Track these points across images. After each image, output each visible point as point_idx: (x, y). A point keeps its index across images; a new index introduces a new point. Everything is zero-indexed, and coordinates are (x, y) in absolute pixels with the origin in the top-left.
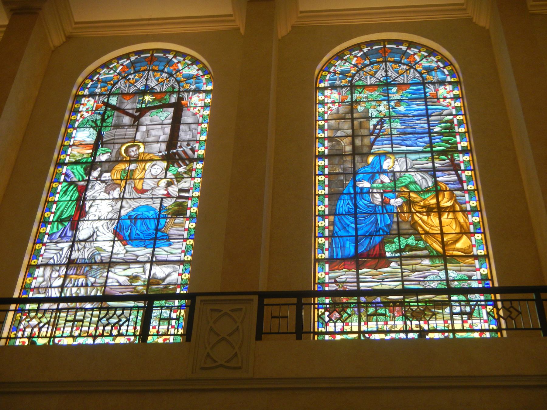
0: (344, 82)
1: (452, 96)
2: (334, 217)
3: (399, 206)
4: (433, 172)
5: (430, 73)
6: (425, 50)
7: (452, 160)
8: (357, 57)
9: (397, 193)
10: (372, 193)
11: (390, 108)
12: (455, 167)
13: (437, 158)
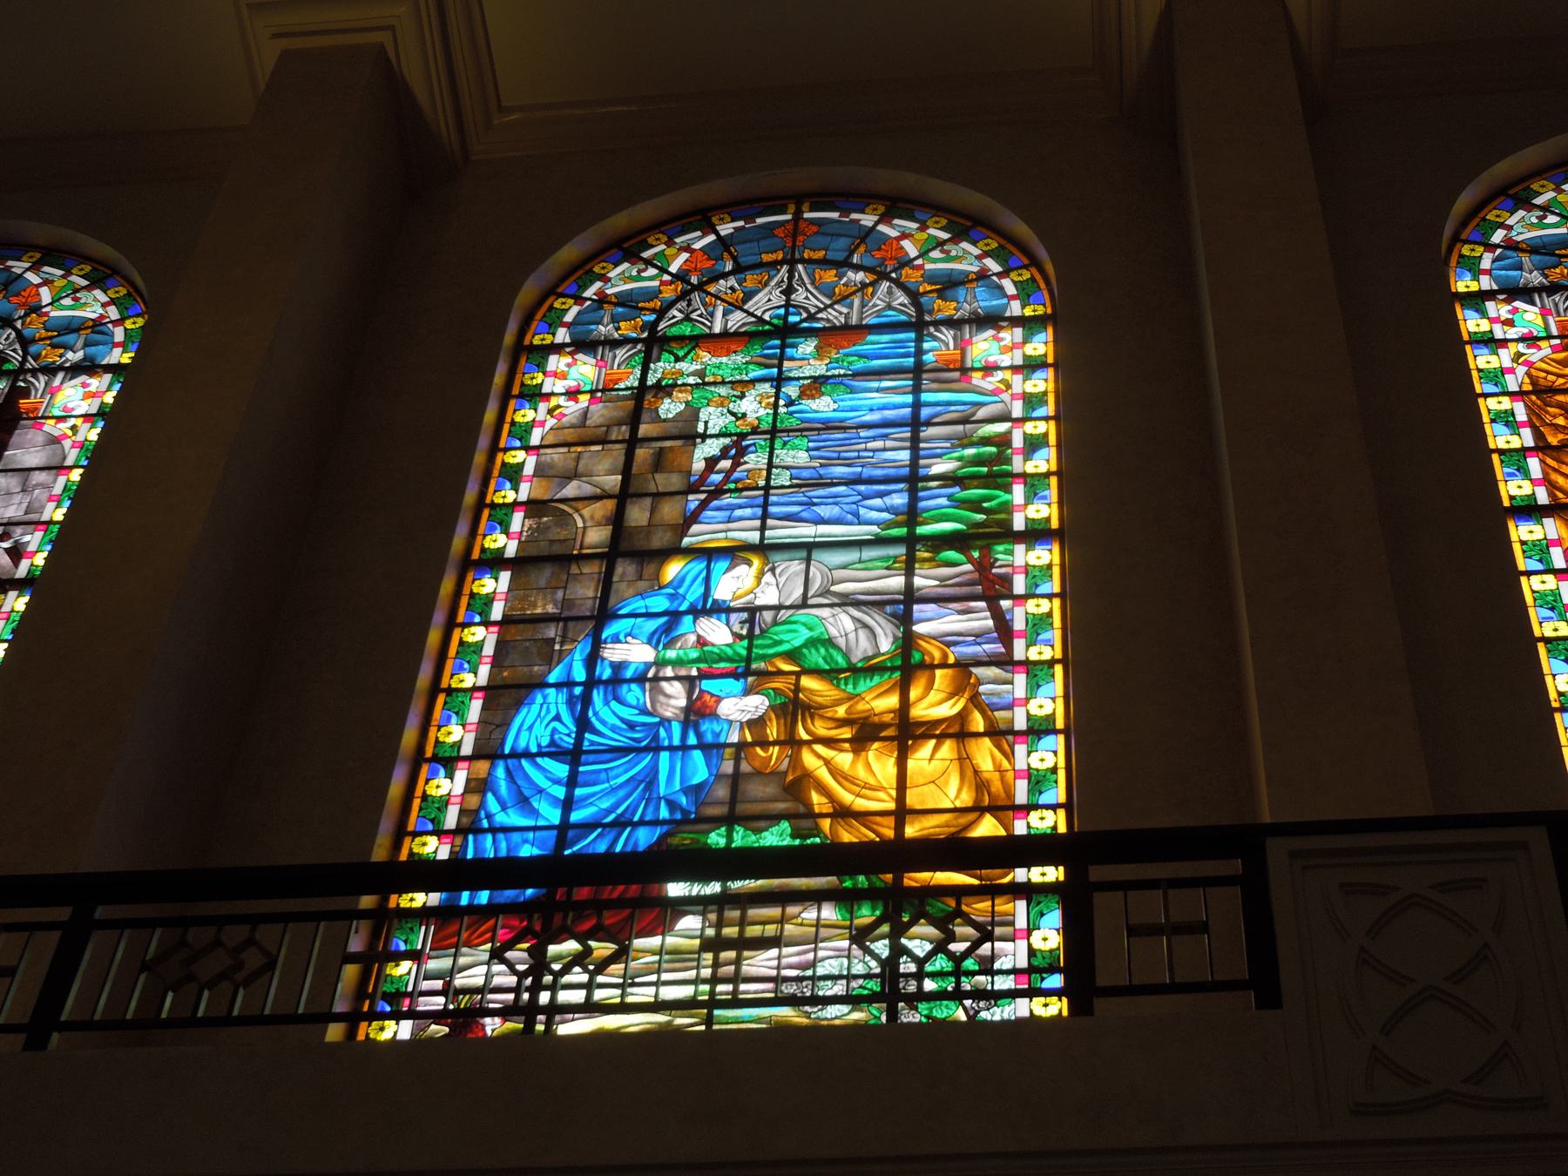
0: (626, 329)
1: (1019, 361)
4: (903, 607)
5: (949, 293)
6: (944, 222)
7: (984, 566)
8: (692, 251)
9: (750, 679)
11: (782, 402)
13: (925, 560)
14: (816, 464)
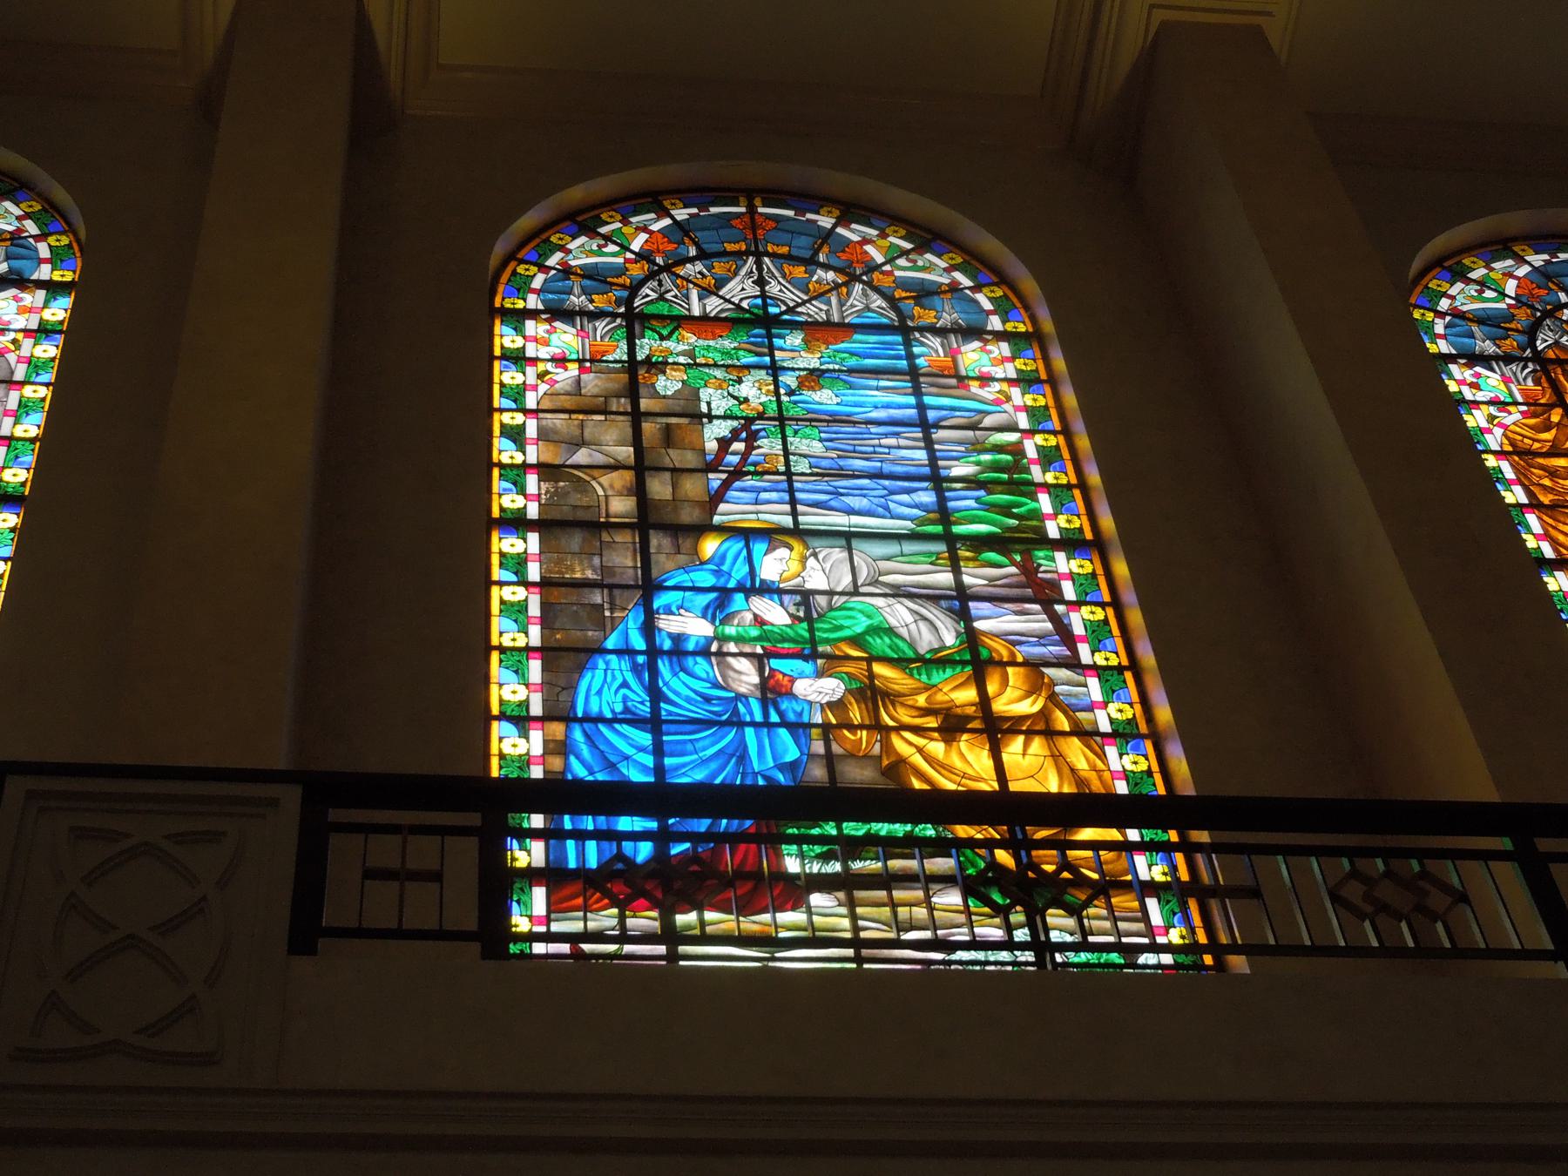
0: (600, 302)
2: (567, 726)
3: (830, 705)
4: (959, 602)
5: (925, 301)
9: (820, 662)
10: (721, 654)
11: (782, 391)
12: (1045, 594)
13: (968, 559)
14: (833, 454)
